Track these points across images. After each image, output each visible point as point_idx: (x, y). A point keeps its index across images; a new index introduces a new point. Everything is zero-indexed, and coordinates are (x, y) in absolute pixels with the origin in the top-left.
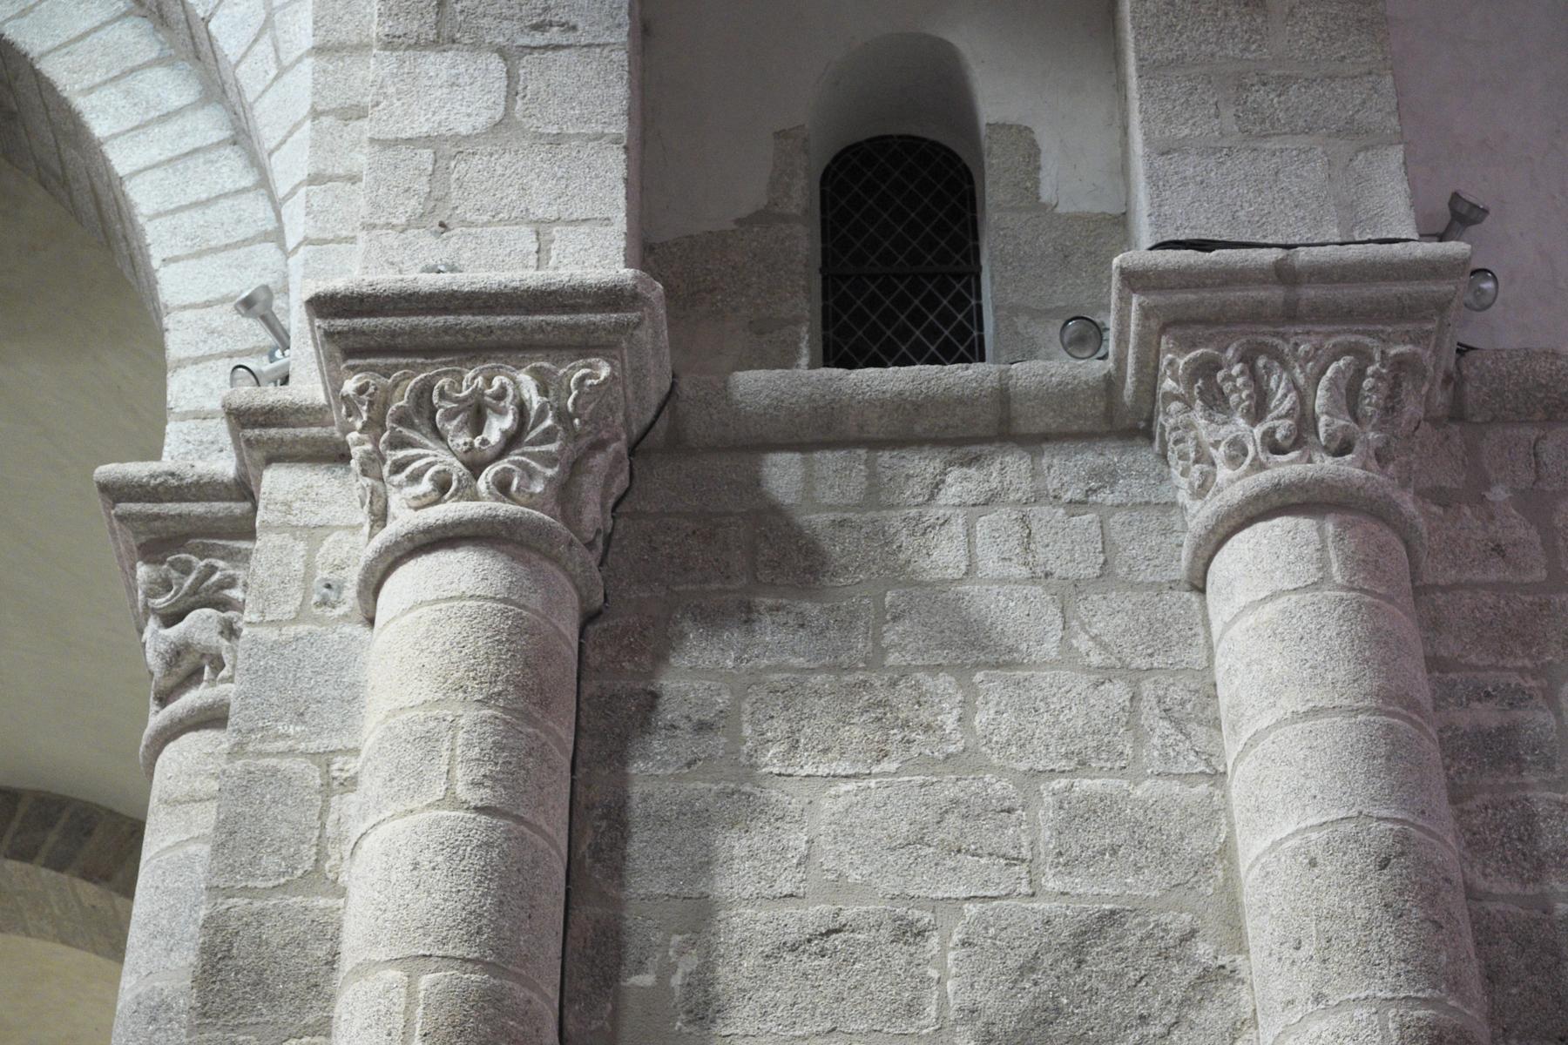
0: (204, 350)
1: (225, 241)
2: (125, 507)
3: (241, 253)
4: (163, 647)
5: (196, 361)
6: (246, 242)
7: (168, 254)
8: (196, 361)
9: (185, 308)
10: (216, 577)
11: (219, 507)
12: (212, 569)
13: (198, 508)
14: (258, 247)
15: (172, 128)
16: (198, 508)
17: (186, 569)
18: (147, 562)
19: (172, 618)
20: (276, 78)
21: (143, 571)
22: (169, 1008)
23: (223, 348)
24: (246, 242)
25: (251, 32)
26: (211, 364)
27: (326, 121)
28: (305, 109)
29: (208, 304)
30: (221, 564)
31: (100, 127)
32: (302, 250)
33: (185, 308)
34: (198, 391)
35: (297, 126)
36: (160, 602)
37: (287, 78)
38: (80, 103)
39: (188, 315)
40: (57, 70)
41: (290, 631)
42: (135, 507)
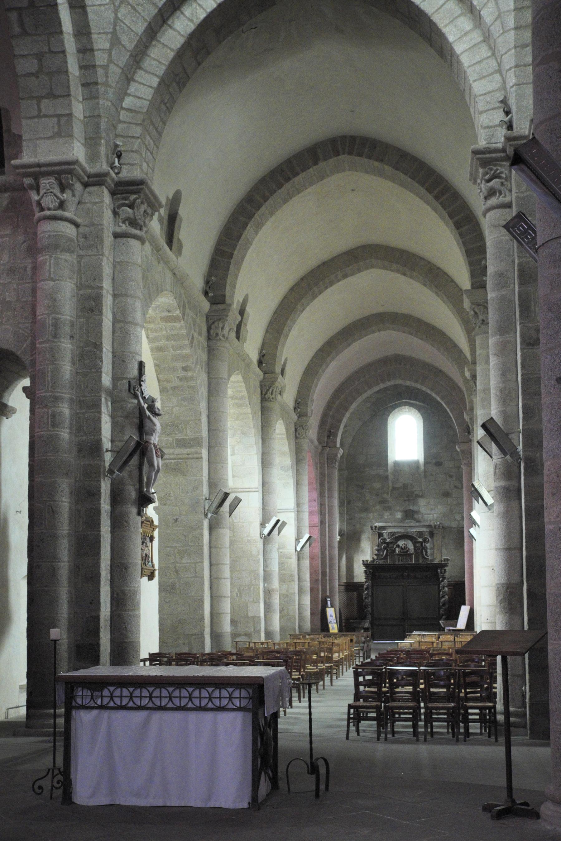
0: (487, 108)
1: (487, 74)
2: (478, 156)
3: (491, 77)
4: (487, 188)
5: (486, 111)
6: (492, 74)
7: (474, 79)
8: (486, 111)
9: (480, 95)
10: (498, 171)
11: (499, 155)
12: (497, 170)
13: (494, 155)
14: (495, 75)
15: (468, 38)
16: (494, 155)
17: (491, 169)
18: (482, 168)
19: (488, 181)
20: (502, 33)
21: (481, 171)
22: (503, 274)
23: (490, 107)
24: (492, 74)
25: (494, 17)
26: (489, 112)
27: (518, 49)
28: (512, 45)
29: (485, 94)
30: (499, 168)
31: (451, 38)
32: (514, 87)
33: (480, 95)
34: (487, 120)
35: (510, 50)
36: (487, 177)
37: (506, 34)
38: (444, 30)
39: (481, 98)
40: (436, 18)
41: (526, 194)
42: (480, 156)
